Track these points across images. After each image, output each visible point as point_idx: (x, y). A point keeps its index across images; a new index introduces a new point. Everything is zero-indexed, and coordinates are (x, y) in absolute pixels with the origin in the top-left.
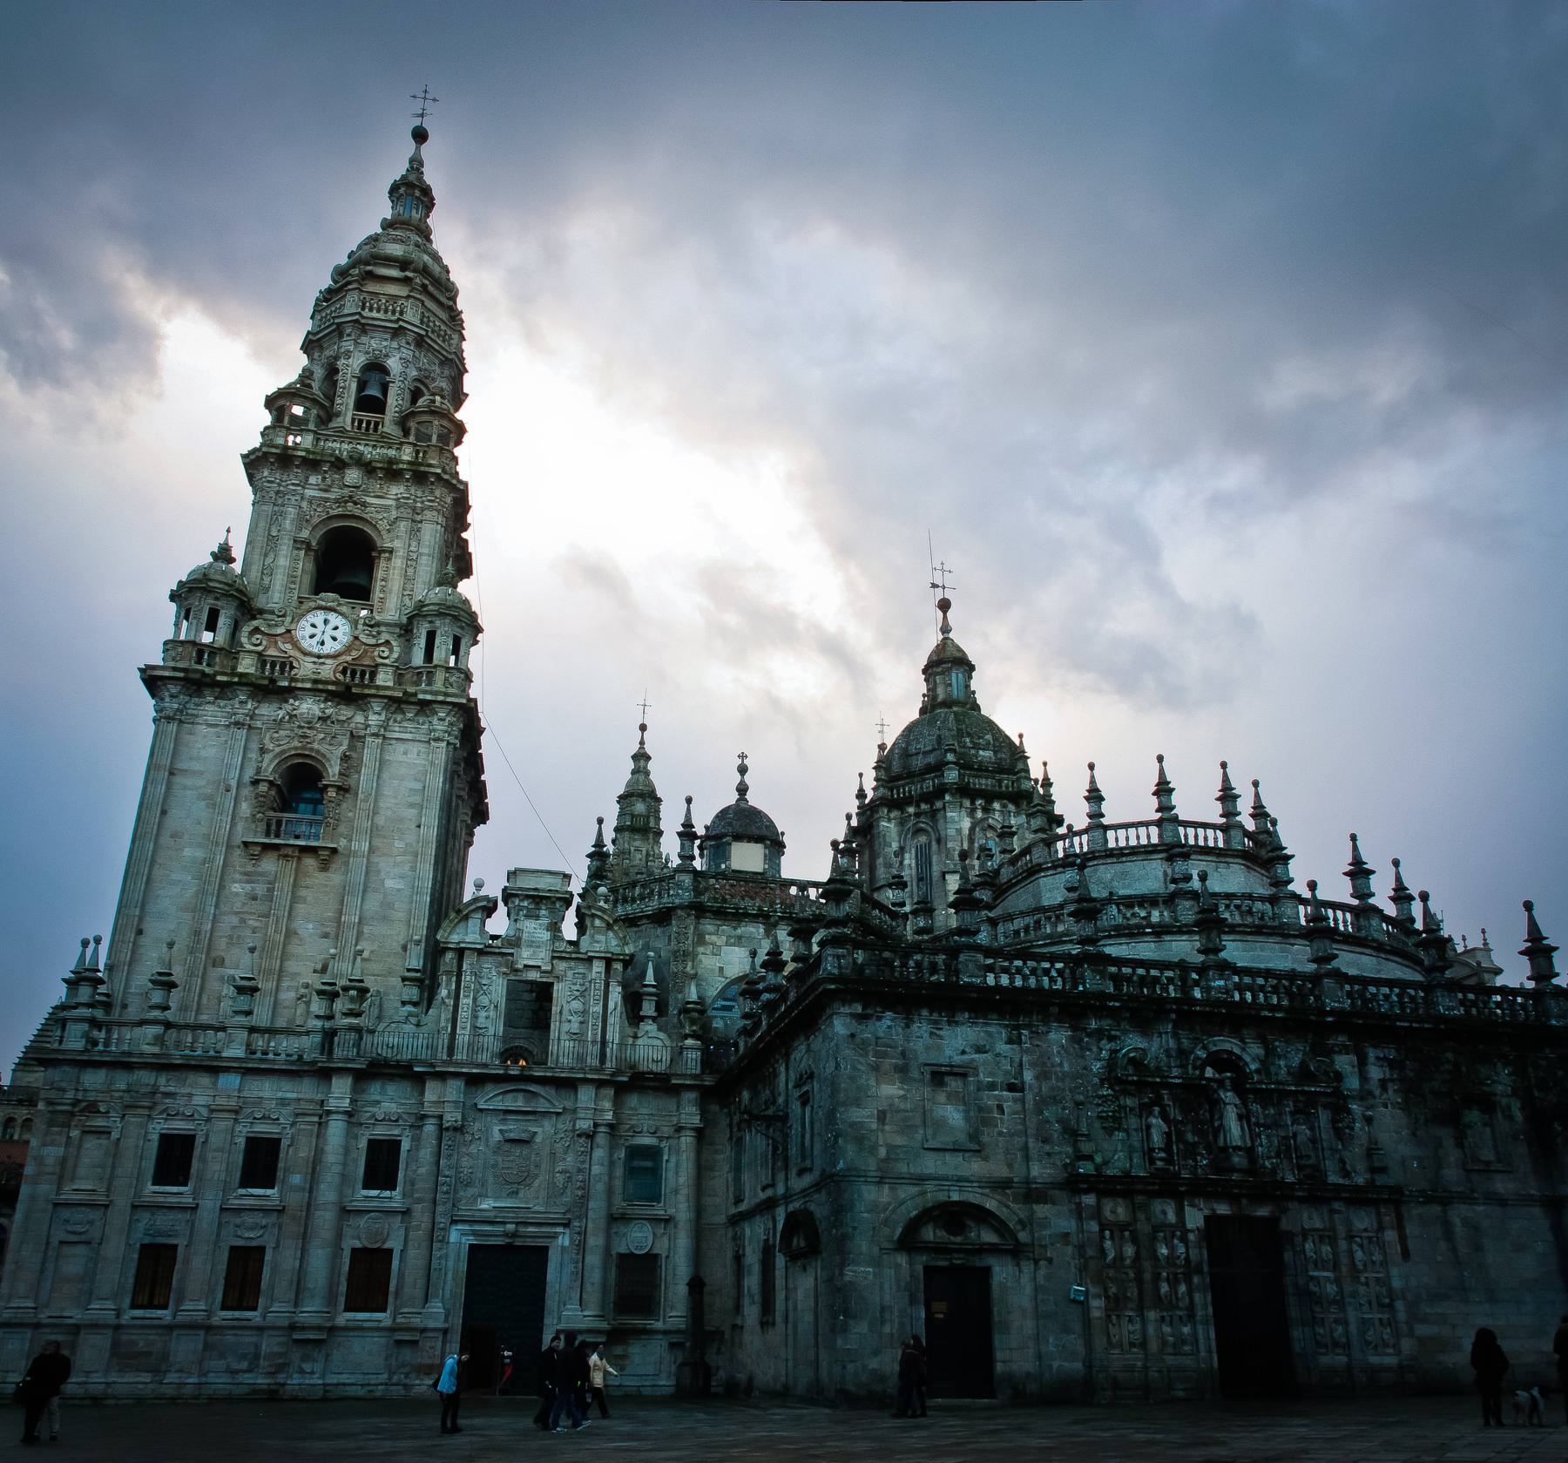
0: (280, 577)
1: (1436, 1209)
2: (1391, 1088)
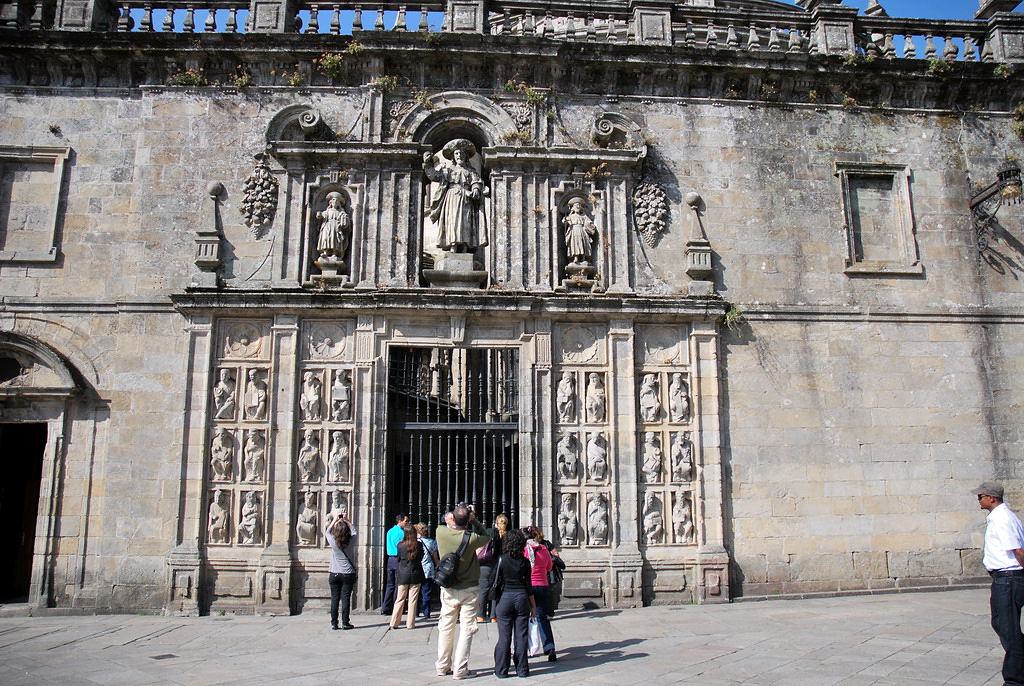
1: (792, 329)
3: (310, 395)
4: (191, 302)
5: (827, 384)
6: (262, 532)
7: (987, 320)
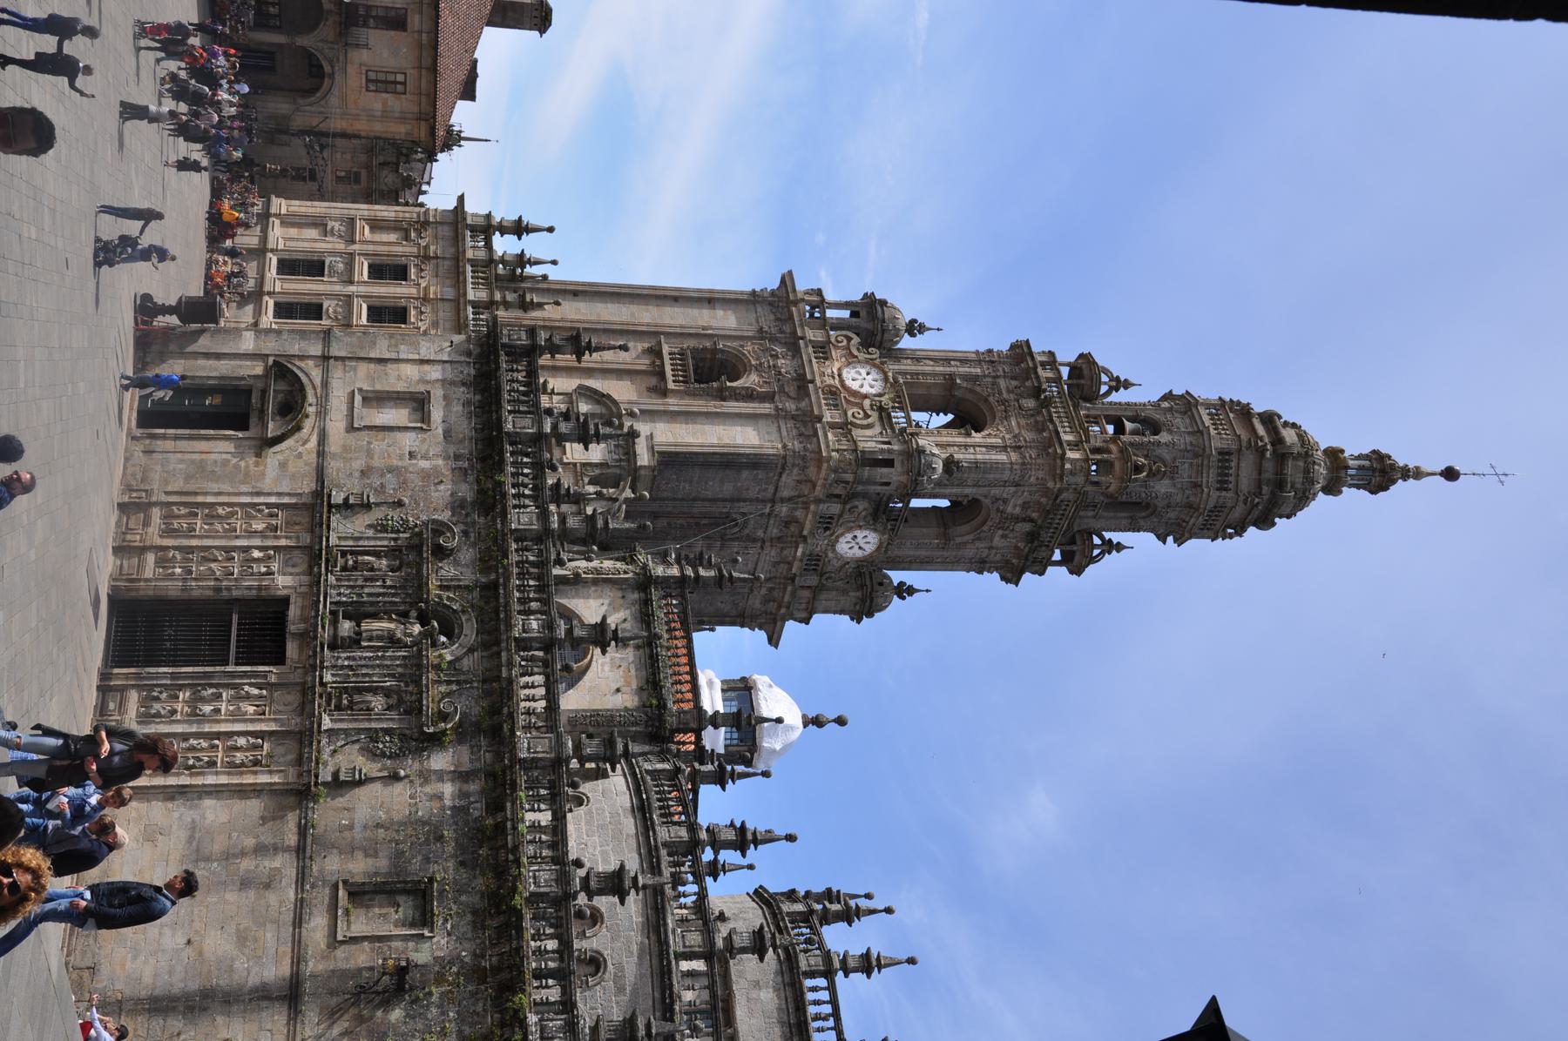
0: (913, 368)
1: (292, 839)
2: (436, 805)
3: (256, 554)
4: (320, 494)
5: (246, 864)
6: (169, 532)
7: (291, 995)
